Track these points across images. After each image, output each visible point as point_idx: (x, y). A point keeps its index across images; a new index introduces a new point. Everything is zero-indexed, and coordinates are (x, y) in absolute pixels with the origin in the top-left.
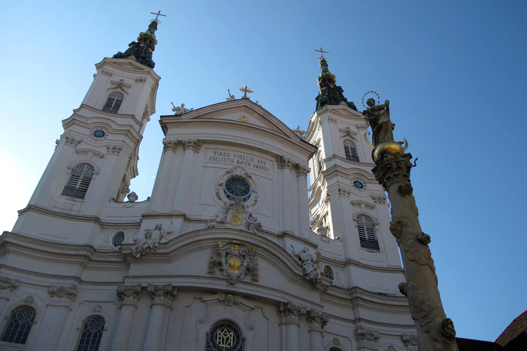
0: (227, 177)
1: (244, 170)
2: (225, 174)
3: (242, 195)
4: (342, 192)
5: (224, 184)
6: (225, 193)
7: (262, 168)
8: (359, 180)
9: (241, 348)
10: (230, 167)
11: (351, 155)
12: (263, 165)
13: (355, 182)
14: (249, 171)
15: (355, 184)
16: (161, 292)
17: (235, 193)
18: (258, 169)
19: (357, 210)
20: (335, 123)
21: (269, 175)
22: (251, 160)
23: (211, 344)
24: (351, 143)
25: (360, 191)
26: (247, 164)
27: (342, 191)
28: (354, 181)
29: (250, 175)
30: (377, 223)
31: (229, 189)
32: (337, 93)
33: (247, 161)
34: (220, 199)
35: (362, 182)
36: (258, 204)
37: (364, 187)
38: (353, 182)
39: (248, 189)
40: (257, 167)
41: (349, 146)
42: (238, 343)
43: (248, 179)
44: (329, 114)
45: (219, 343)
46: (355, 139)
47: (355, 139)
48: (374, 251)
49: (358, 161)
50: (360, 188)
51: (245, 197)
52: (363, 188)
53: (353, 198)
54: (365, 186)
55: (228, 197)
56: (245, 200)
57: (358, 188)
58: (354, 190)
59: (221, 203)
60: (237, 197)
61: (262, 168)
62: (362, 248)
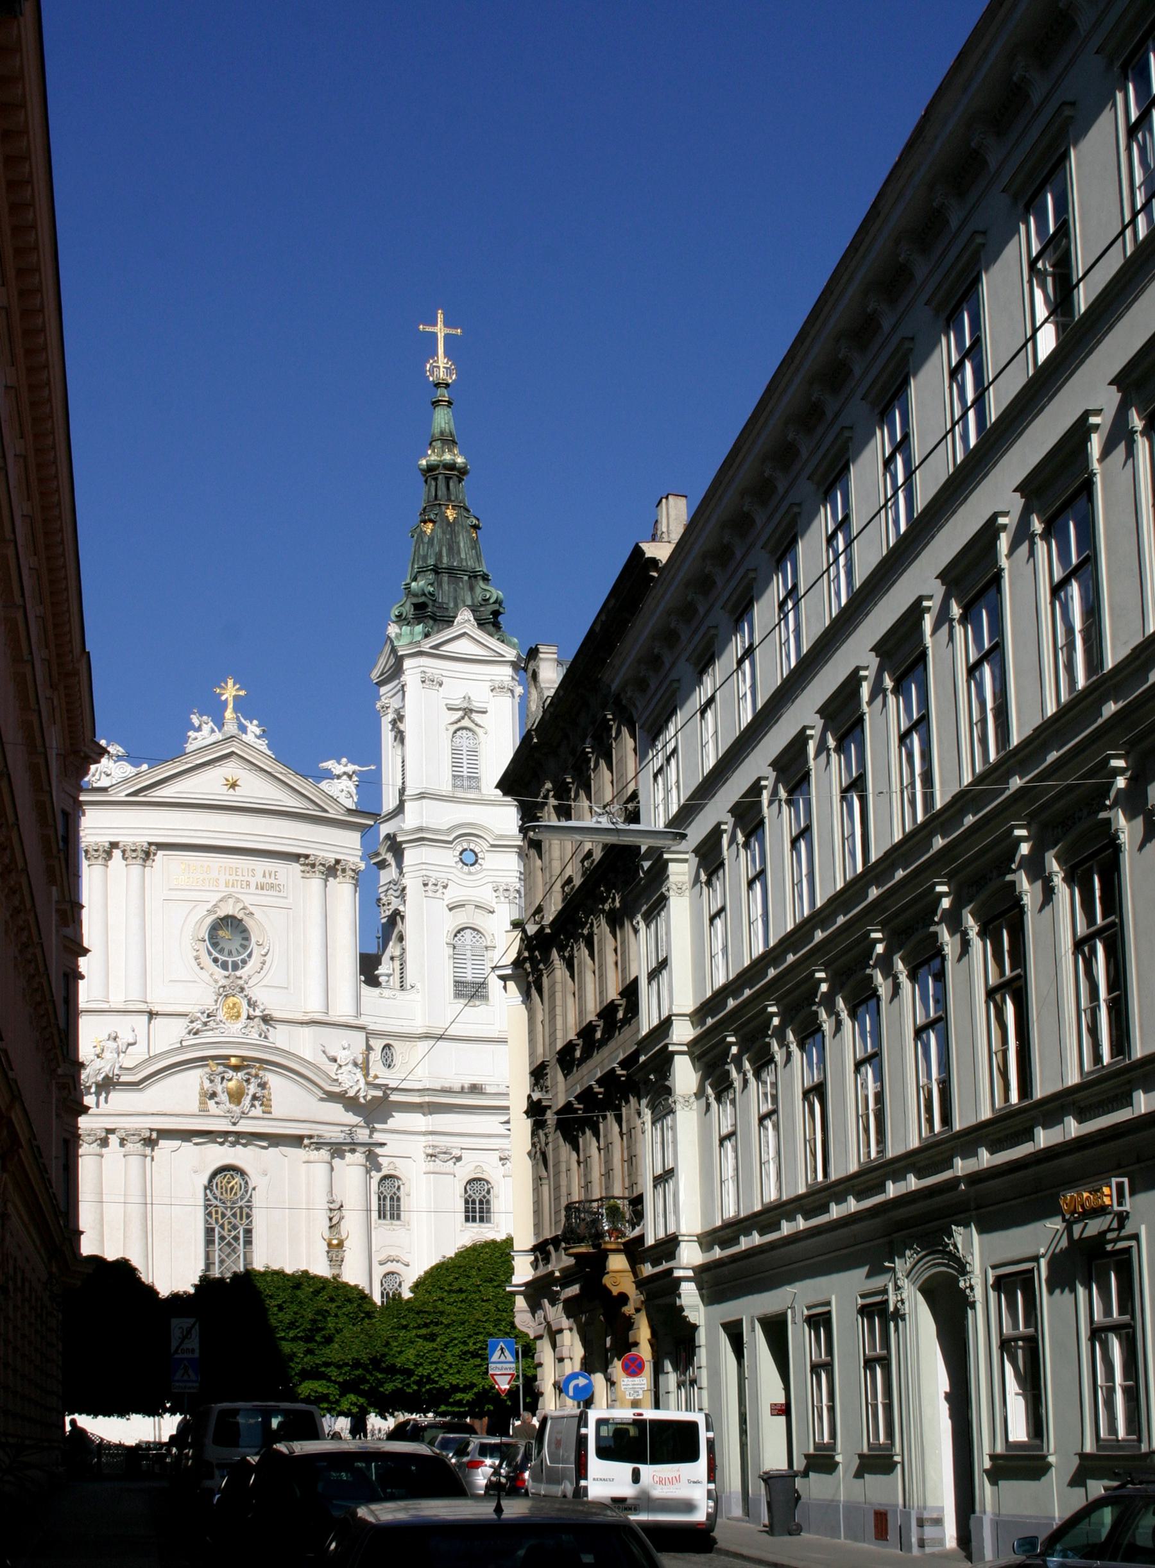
0: (210, 920)
1: (238, 900)
2: (206, 916)
3: (239, 953)
4: (430, 887)
5: (206, 938)
6: (210, 954)
7: (272, 886)
8: (472, 846)
9: (251, 1197)
10: (214, 898)
11: (465, 770)
12: (272, 880)
13: (461, 854)
14: (248, 900)
15: (463, 857)
16: (137, 1138)
17: (226, 952)
18: (264, 892)
19: (461, 918)
20: (437, 688)
21: (286, 898)
22: (251, 873)
23: (210, 1196)
24: (470, 734)
25: (470, 873)
26: (244, 886)
27: (430, 884)
28: (461, 849)
29: (252, 909)
30: (492, 945)
31: (215, 945)
32: (462, 545)
33: (243, 878)
34: (202, 968)
35: (476, 850)
36: (266, 967)
37: (480, 861)
38: (458, 853)
39: (247, 939)
40: (262, 889)
41: (465, 742)
42: (247, 1192)
43: (246, 918)
44: (423, 660)
45: (222, 1194)
46: (480, 726)
47: (480, 726)
48: (478, 1003)
49: (478, 788)
50: (472, 865)
51: (242, 957)
52: (477, 866)
53: (453, 894)
54: (483, 859)
55: (215, 960)
56: (244, 962)
57: (467, 865)
58: (458, 873)
59: (204, 975)
60: (230, 960)
61: (272, 886)
62: (456, 1001)
